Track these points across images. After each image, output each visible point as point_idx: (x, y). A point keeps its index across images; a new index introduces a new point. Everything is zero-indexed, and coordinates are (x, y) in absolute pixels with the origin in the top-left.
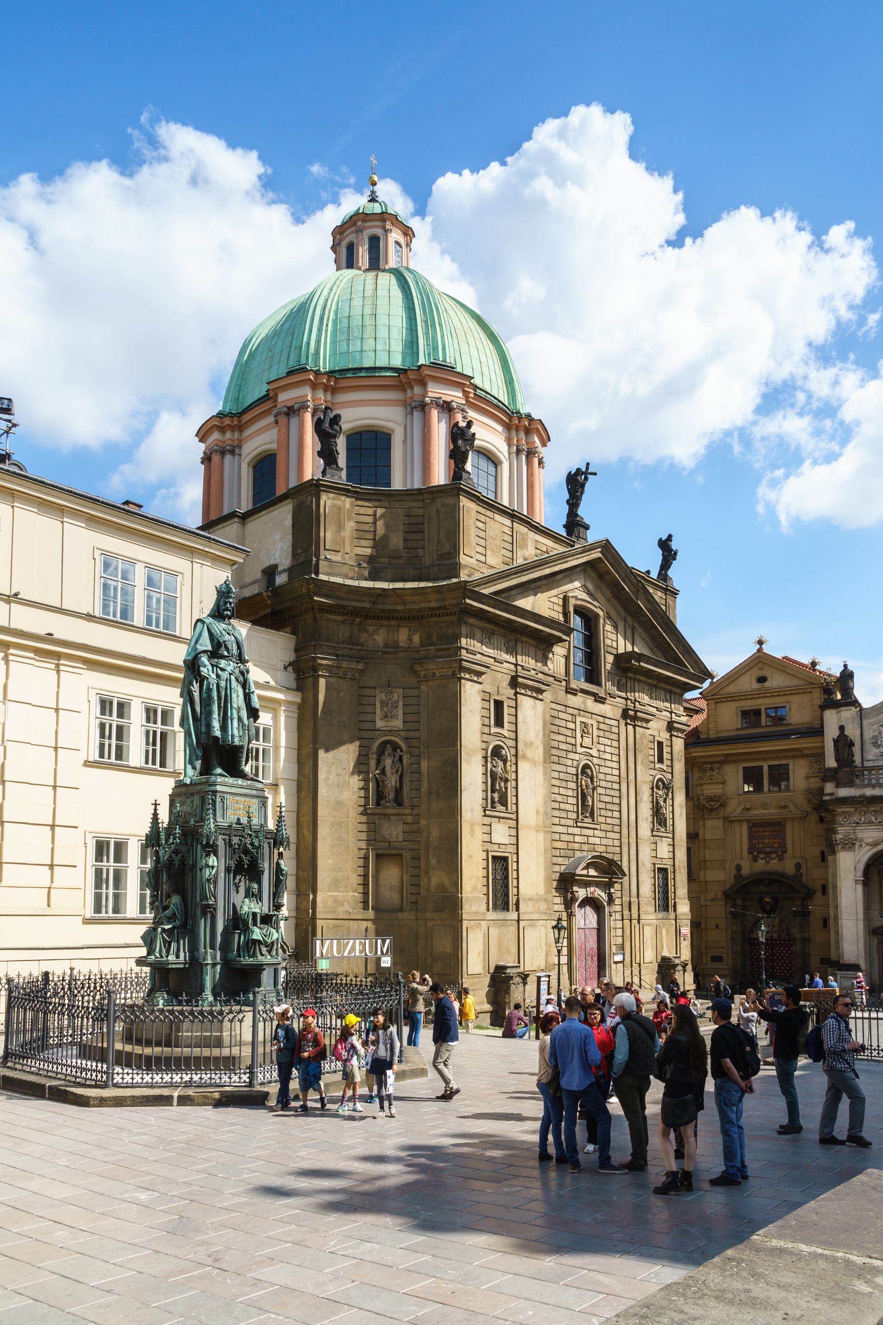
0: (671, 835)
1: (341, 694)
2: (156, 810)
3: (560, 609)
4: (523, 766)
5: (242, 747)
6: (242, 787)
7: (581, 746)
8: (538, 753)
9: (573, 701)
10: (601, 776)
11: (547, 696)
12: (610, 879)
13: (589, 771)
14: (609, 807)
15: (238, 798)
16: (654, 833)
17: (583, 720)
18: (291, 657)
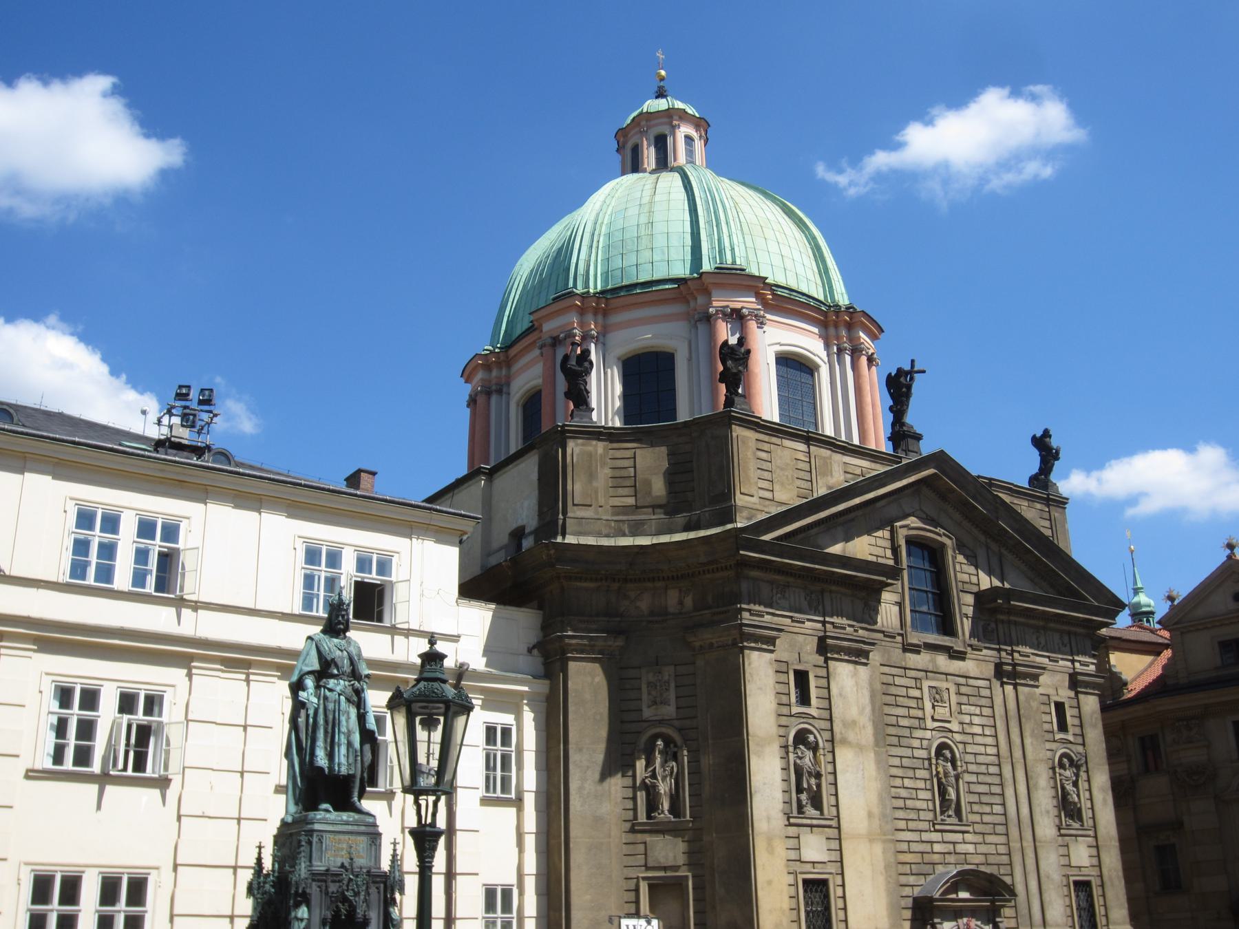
0: (1091, 833)
2: (260, 853)
3: (888, 544)
4: (844, 756)
5: (353, 776)
6: (347, 823)
7: (933, 719)
8: (867, 734)
9: (913, 660)
10: (970, 758)
11: (875, 657)
12: (993, 902)
13: (947, 753)
14: (985, 799)
15: (342, 837)
16: (1063, 832)
17: (933, 684)
18: (533, 637)
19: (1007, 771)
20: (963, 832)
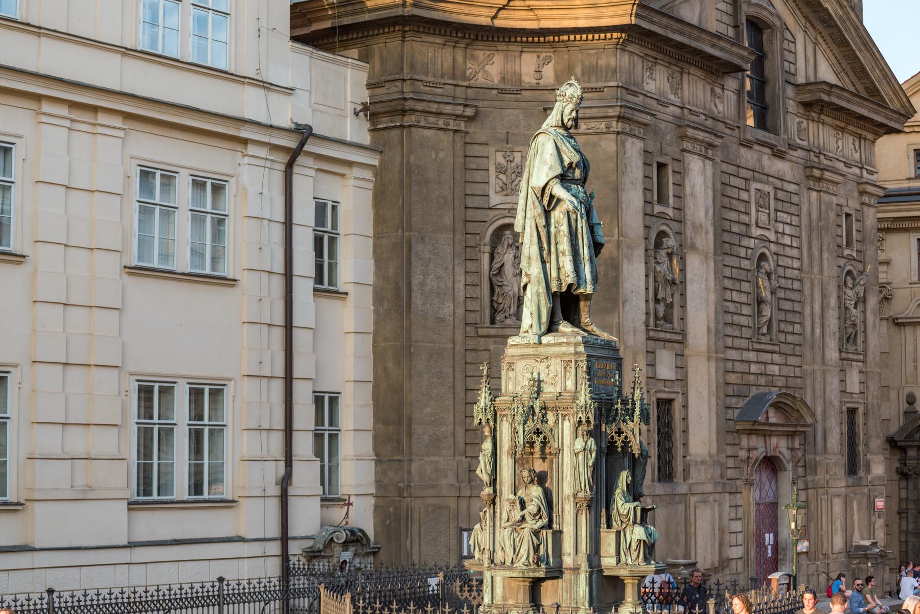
1: (442, 155)
4: (694, 263)
7: (757, 226)
9: (747, 156)
10: (781, 271)
14: (790, 317)
16: (843, 355)
19: (807, 285)
20: (773, 352)
